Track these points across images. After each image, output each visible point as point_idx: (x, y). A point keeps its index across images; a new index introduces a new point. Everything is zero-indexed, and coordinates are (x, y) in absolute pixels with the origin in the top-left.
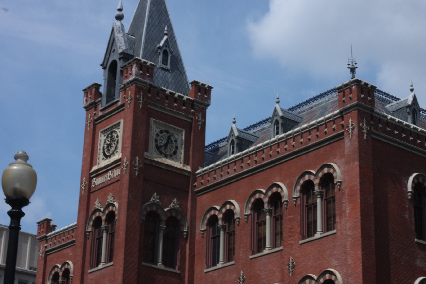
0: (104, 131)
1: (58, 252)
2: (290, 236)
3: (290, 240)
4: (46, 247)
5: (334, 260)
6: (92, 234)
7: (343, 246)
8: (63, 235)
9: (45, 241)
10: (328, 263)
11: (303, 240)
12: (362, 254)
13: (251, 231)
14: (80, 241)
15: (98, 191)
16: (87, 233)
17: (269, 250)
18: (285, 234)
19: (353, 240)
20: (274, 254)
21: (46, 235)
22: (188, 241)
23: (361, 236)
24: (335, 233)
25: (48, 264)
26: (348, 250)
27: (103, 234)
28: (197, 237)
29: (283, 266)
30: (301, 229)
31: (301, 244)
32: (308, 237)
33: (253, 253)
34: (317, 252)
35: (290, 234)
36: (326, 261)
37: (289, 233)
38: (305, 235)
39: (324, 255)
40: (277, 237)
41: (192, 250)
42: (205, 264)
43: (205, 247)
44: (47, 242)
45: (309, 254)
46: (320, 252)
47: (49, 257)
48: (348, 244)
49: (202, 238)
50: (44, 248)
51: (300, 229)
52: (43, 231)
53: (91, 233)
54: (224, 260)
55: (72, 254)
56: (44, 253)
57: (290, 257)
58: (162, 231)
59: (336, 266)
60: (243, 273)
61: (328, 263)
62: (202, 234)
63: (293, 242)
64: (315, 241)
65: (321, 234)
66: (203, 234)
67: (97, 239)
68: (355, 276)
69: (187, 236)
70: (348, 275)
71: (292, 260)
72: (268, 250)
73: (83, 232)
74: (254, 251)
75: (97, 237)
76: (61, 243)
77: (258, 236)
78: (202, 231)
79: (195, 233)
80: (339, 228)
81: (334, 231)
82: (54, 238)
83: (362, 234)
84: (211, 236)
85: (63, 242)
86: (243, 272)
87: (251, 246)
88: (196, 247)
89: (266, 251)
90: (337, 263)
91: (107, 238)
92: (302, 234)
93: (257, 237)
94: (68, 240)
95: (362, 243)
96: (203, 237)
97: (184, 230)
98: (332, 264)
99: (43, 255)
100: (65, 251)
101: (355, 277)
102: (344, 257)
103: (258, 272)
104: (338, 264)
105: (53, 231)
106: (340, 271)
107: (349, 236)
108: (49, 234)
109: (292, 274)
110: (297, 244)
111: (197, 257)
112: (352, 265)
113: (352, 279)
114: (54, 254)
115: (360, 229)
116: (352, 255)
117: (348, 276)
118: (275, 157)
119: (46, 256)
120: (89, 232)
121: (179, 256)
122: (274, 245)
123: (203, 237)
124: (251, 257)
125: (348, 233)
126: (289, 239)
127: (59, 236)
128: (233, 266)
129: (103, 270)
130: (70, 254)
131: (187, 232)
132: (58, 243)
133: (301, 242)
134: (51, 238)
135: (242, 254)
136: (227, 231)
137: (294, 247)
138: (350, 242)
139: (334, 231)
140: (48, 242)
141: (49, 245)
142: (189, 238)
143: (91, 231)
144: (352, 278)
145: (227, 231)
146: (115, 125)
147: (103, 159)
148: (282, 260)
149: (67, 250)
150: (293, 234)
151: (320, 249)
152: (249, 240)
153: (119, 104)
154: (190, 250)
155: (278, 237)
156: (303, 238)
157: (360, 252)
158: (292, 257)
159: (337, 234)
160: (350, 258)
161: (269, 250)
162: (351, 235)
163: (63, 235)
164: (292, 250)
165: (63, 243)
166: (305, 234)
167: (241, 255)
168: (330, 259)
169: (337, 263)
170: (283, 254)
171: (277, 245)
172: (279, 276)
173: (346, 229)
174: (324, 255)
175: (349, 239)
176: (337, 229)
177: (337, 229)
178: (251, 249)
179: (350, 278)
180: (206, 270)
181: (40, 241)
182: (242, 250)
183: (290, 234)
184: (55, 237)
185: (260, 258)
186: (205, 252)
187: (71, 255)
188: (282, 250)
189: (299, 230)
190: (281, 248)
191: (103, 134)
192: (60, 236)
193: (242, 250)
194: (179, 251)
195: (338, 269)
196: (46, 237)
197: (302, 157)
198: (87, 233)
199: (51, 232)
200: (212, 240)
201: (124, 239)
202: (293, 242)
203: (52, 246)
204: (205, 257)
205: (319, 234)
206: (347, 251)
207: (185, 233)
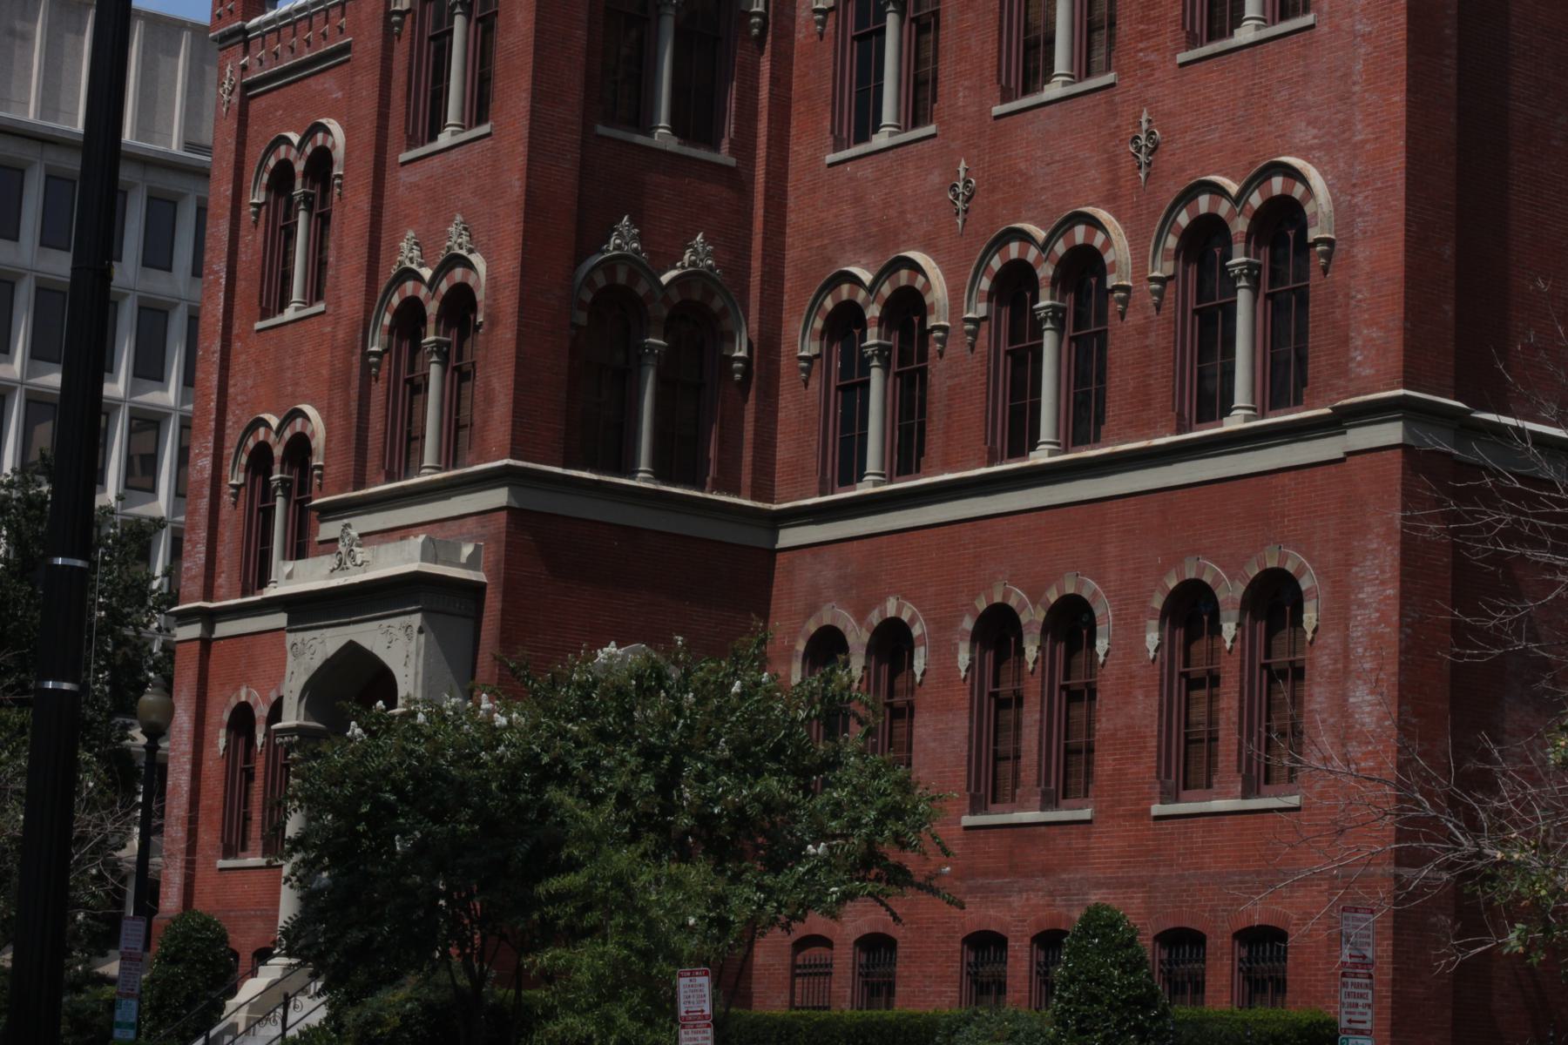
1: (286, 88)
2: (1144, 36)
3: (1141, 50)
4: (244, 68)
5: (1304, 124)
6: (413, 22)
7: (1339, 74)
8: (305, 23)
9: (239, 48)
10: (1280, 136)
11: (1192, 49)
12: (1407, 105)
13: (1001, 12)
14: (368, 44)
16: (395, 18)
17: (1065, 84)
18: (1124, 28)
19: (1375, 54)
20: (1085, 99)
21: (244, 26)
22: (768, 47)
23: (1405, 37)
24: (1312, 27)
25: (252, 130)
26: (1357, 88)
27: (452, 22)
28: (800, 36)
29: (1114, 146)
30: (1184, 11)
31: (1182, 65)
32: (1211, 39)
33: (1005, 99)
34: (1241, 93)
35: (1142, 27)
36: (1272, 128)
37: (1142, 22)
38: (1197, 30)
39: (1266, 105)
40: (1096, 36)
41: (781, 81)
42: (828, 135)
43: (830, 72)
44: (246, 52)
45: (1213, 101)
46: (1252, 95)
47: (255, 106)
48: (1359, 67)
49: (816, 37)
50: (238, 73)
51: (1181, 7)
52: (231, 11)
53: (409, 17)
54: (898, 120)
55: (339, 95)
56: (238, 89)
57: (1142, 111)
58: (671, 11)
59: (1312, 148)
60: (967, 170)
61: (1280, 136)
62: (818, 22)
63: (1152, 57)
65: (1258, 28)
66: (823, 23)
67: (431, 38)
68: (1379, 185)
69: (763, 29)
70: (1354, 181)
71: (1149, 121)
72: (1060, 83)
73: (381, 11)
74: (1011, 89)
75: (429, 31)
76: (301, 53)
77: (1026, 32)
78: (817, 11)
79: (793, 20)
80: (1326, 8)
81: (1309, 19)
82: (274, 36)
83: (1409, 30)
84: (851, 31)
85: (306, 50)
86: (966, 164)
87: (999, 70)
88: (795, 72)
89: (1053, 90)
90: (1315, 138)
91: (467, 34)
92: (1188, 29)
93: (1022, 38)
94: (323, 43)
95: (1409, 66)
96: (821, 36)
97: (752, 7)
98: (1297, 140)
99: (235, 99)
100: (311, 81)
101: (1377, 189)
102: (1341, 116)
103: (1023, 166)
104: (1316, 141)
105: (268, 9)
106: (1326, 168)
107: (1363, 36)
108: (255, 21)
109: (1148, 175)
110: (1171, 66)
111: (798, 109)
112: (1368, 146)
113: (1366, 197)
114: (275, 93)
115: (1405, 11)
116: (1371, 110)
117: (1354, 185)
119: (245, 102)
120: (402, 14)
121: (732, 105)
122: (1084, 66)
123: (821, 36)
124: (998, 110)
125: (1359, 27)
126: (1141, 45)
127: (290, 30)
128: (931, 141)
129: (453, 154)
130: (334, 96)
131: (764, 16)
132: (287, 54)
133: (1182, 57)
134: (263, 36)
135: (964, 97)
136: (911, 14)
137: (1157, 74)
138: (1365, 60)
139: (1309, 19)
140: (252, 50)
141: (258, 63)
142: (769, 38)
143: (408, 11)
144: (1366, 193)
145: (911, 14)
148: (1113, 125)
149: (321, 78)
150: (1153, 27)
151: (1254, 84)
152: (991, 48)
154: (774, 80)
155: (1100, 37)
156: (1193, 41)
157: (1399, 98)
158: (1150, 114)
159: (1317, 29)
160: (1361, 121)
161: (1065, 84)
162: (1370, 33)
163: (305, 23)
164: (1152, 85)
165: (307, 55)
166: (1200, 26)
167: (960, 104)
168: (1289, 121)
169: (1315, 137)
170: (1117, 99)
171: (1094, 66)
172: (1098, 181)
173: (1350, 13)
174: (1266, 105)
175: (1362, 51)
176: (1319, 11)
177: (1319, 11)
178: (999, 80)
179: (1360, 193)
180: (831, 158)
181: (222, 46)
182: (966, 83)
183: (1142, 27)
184: (277, 30)
185: (1030, 114)
186: (830, 91)
187: (337, 100)
188: (1112, 85)
189: (1178, 11)
192: (295, 29)
193: (966, 83)
194: (735, 84)
195: (1319, 158)
196: (243, 32)
198: (395, 18)
199: (264, 12)
200: (856, 44)
201: (531, 40)
202: (1152, 57)
203: (265, 64)
204: (829, 109)
205: (1253, 27)
206: (1354, 93)
207: (756, 20)
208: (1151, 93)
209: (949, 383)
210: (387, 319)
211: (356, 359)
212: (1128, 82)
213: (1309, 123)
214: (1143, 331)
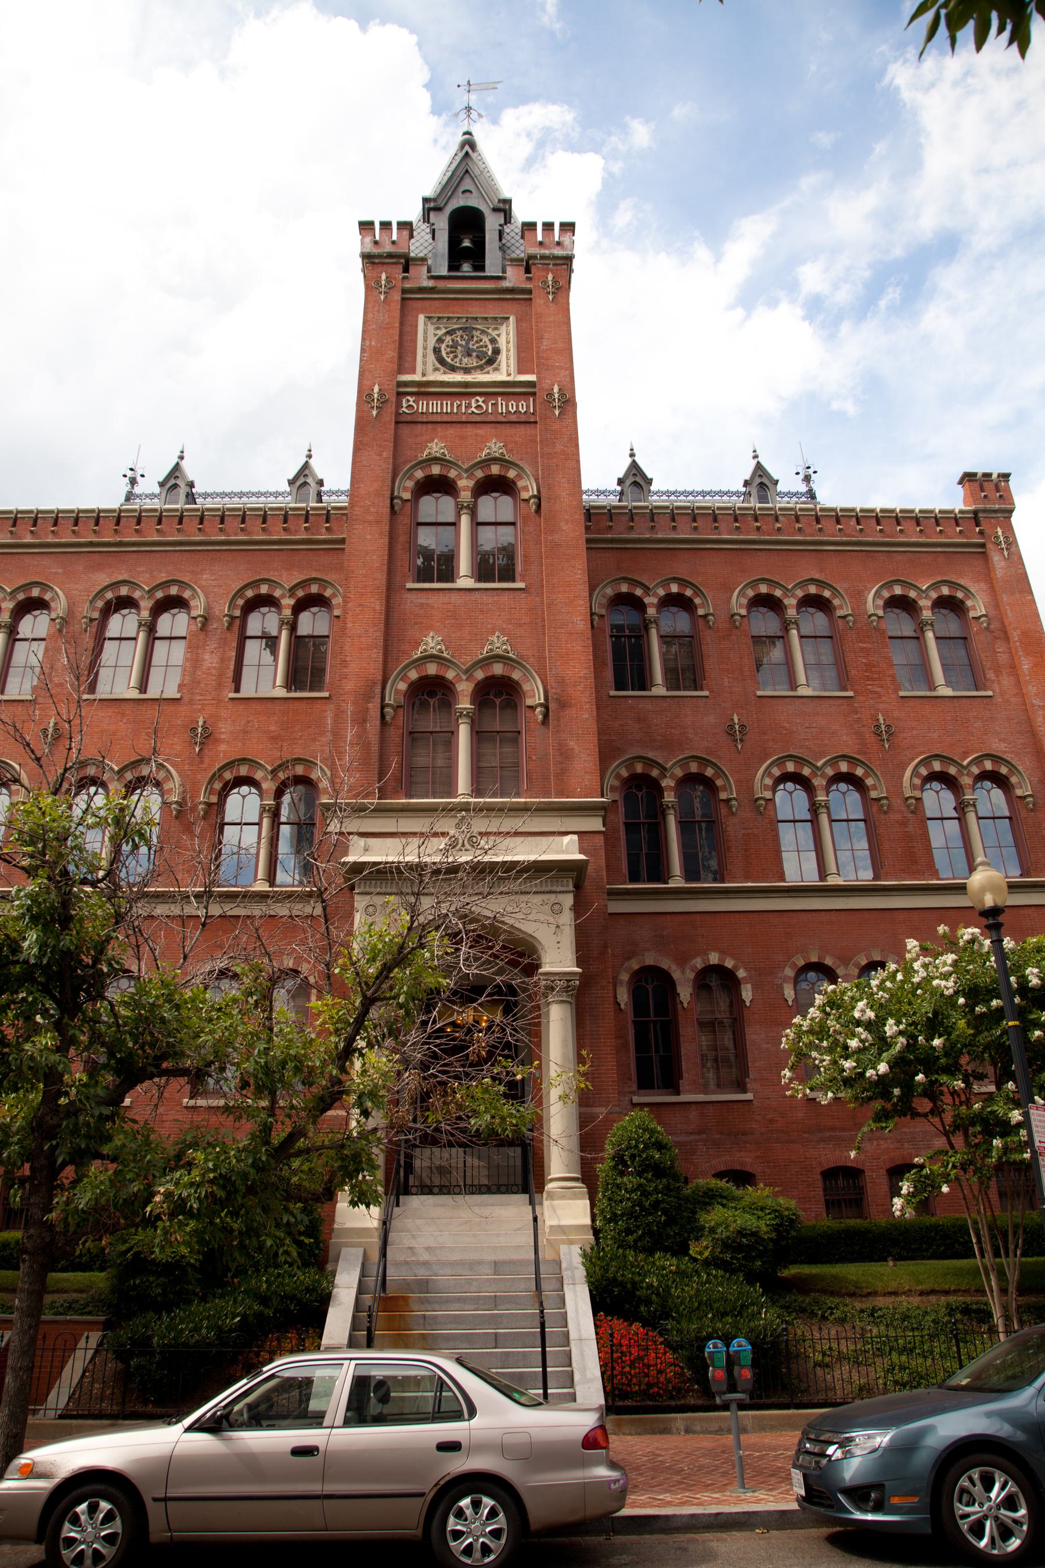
0: (439, 318)
15: (430, 426)
63: (879, 689)
64: (938, 700)
103: (787, 725)
118: (813, 535)
128: (704, 700)
129: (477, 595)
133: (901, 694)
139: (990, 693)
146: (486, 319)
147: (436, 369)
153: (506, 284)
180: (613, 693)
185: (787, 700)
190: (850, 694)
191: (432, 324)
197: (877, 555)
202: (879, 689)
208: (881, 706)
209: (743, 832)
210: (403, 686)
211: (374, 707)
212: (861, 698)
213: (1000, 740)
214: (904, 823)
